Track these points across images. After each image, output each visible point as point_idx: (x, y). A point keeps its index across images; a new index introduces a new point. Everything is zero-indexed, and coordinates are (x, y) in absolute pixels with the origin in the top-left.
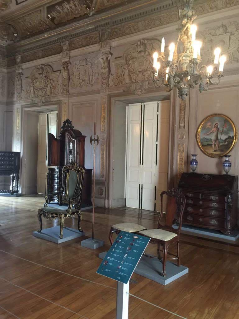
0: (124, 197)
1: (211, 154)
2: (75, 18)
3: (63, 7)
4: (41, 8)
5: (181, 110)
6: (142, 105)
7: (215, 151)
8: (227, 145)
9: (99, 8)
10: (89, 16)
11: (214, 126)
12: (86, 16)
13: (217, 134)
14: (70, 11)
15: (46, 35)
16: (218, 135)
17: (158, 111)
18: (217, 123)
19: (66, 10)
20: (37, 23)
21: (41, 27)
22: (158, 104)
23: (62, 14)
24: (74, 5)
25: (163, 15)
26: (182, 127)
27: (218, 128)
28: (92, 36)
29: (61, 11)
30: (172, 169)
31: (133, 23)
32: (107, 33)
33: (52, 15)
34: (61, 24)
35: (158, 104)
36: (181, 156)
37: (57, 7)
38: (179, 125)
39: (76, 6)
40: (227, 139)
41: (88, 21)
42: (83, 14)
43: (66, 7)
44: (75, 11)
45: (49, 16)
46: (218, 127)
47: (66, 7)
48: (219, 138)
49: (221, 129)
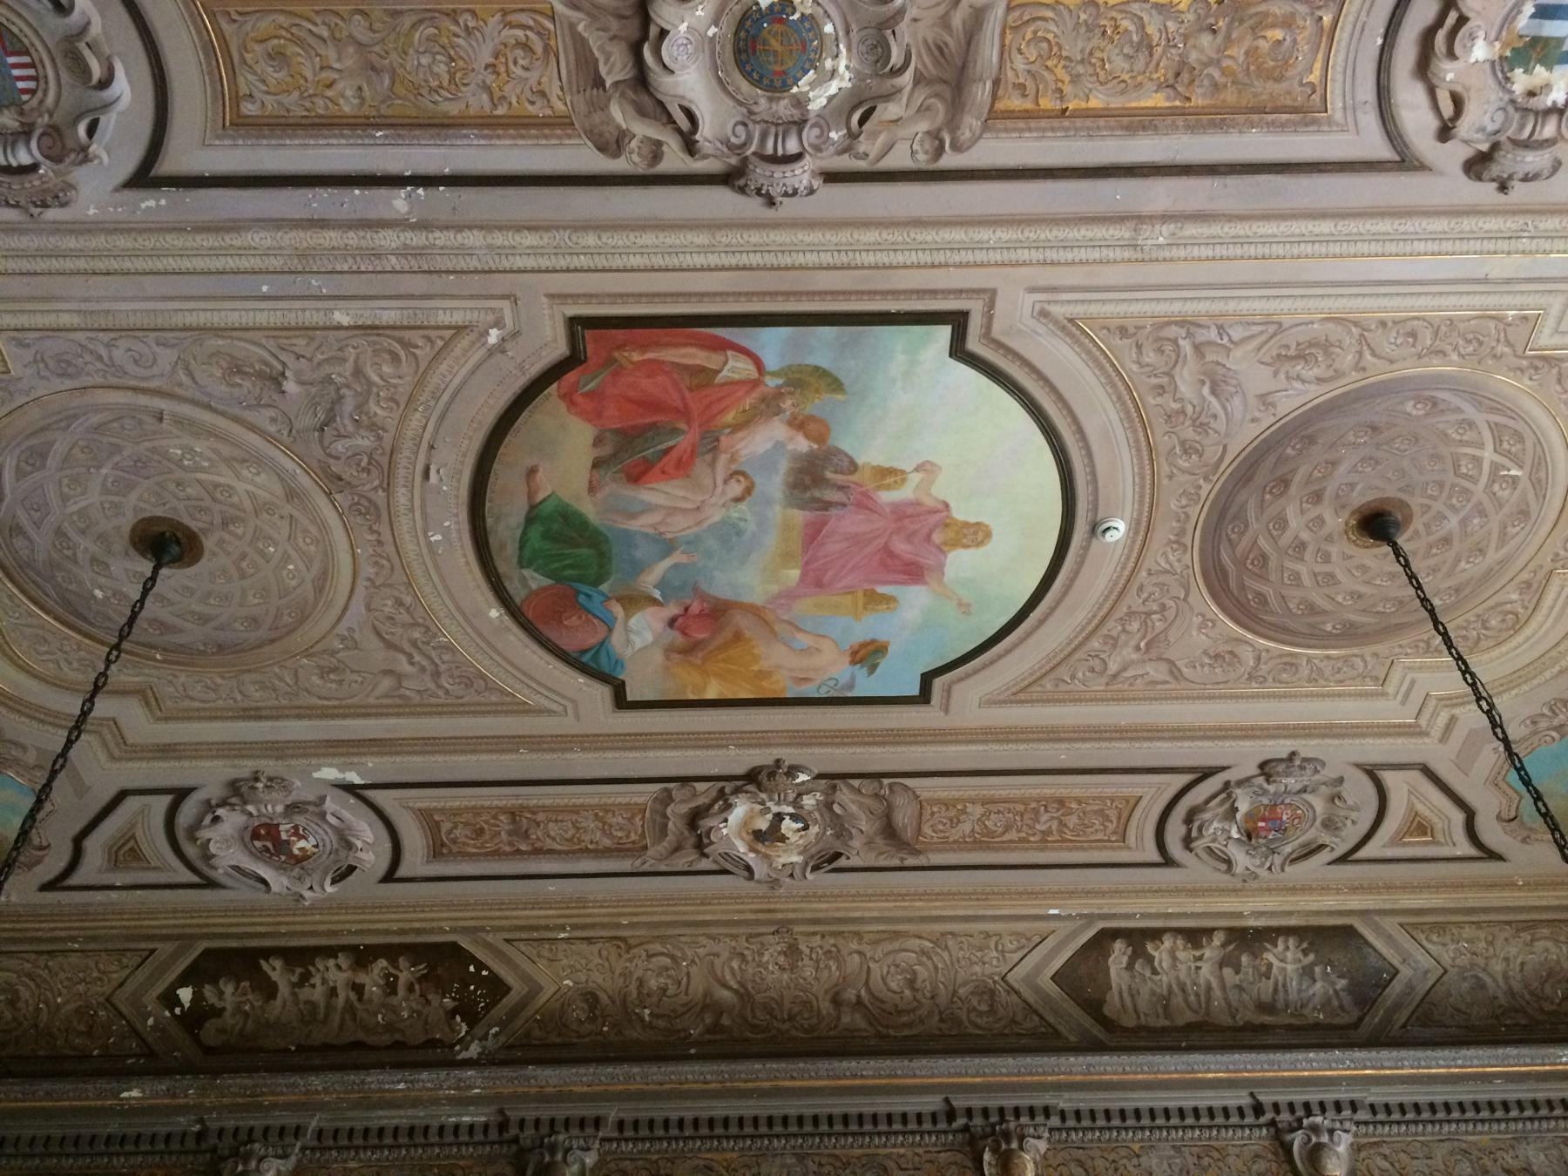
2: (359, 1045)
3: (305, 978)
4: (165, 949)
9: (528, 1034)
10: (459, 1057)
12: (429, 1053)
14: (340, 1001)
15: (135, 1093)
19: (317, 993)
20: (71, 1006)
21: (80, 1034)
23: (279, 1002)
24: (382, 982)
25: (901, 1156)
28: (462, 1163)
29: (284, 990)
31: (735, 1155)
32: (576, 1168)
33: (208, 991)
34: (250, 1053)
37: (275, 970)
39: (391, 987)
41: (479, 1082)
42: (423, 1039)
43: (324, 981)
44: (375, 1015)
45: (185, 994)
47: (324, 981)
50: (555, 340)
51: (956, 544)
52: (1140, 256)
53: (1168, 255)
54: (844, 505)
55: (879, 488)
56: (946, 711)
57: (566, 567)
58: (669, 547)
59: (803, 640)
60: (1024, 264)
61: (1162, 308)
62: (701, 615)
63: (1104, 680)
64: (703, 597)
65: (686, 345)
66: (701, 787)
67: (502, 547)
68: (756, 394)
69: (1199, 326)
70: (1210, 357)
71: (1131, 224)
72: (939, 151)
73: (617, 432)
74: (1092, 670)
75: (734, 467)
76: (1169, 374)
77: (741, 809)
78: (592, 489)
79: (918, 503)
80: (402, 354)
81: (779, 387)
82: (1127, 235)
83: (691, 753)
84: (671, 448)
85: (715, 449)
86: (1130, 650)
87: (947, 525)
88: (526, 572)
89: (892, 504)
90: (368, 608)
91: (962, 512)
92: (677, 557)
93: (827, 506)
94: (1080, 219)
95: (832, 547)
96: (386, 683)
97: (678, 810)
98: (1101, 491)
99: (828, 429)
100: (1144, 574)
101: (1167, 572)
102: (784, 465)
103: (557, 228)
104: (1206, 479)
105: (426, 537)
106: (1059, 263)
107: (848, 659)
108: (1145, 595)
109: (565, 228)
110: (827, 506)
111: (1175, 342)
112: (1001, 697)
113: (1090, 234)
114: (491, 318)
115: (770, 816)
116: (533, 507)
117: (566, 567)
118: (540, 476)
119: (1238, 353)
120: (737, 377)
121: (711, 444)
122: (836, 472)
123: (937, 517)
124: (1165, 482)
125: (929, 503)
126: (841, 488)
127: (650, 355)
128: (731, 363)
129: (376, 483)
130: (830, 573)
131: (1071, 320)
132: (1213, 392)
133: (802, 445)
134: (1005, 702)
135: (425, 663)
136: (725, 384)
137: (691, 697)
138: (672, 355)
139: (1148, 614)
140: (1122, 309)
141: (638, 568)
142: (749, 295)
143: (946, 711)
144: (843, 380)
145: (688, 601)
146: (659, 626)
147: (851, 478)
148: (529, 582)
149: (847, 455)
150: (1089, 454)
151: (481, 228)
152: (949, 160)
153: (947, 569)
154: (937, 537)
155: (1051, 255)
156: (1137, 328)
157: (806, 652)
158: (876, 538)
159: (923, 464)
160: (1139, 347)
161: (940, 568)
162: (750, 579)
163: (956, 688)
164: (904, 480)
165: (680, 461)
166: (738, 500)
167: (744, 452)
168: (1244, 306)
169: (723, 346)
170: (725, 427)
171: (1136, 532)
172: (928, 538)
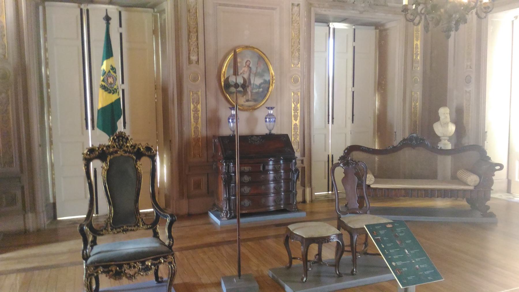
0: (47, 199)
1: (242, 105)
5: (189, 32)
6: (81, 10)
7: (248, 101)
8: (263, 92)
11: (245, 65)
13: (250, 75)
16: (251, 78)
17: (121, 26)
18: (249, 60)
22: (120, 13)
26: (194, 62)
27: (250, 68)
30: (181, 133)
35: (120, 13)
36: (196, 110)
38: (189, 58)
40: (260, 85)
46: (251, 66)
48: (252, 82)
49: (254, 69)
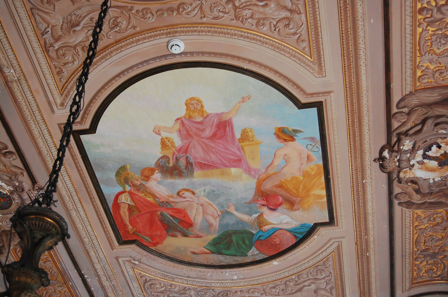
50: (131, 248)
51: (201, 111)
52: (22, 77)
53: (17, 67)
54: (187, 158)
55: (173, 146)
56: (329, 92)
57: (244, 242)
58: (225, 213)
59: (279, 161)
60: (42, 117)
61: (43, 61)
62: (267, 201)
63: (296, 16)
64: (254, 200)
65: (119, 214)
66: (397, 190)
67: (236, 261)
68: (136, 192)
69: (45, 43)
70: (61, 33)
71: (10, 84)
72: (10, 153)
73: (166, 230)
74: (287, 25)
75: (175, 196)
76: (75, 47)
77: (419, 173)
78: (198, 237)
79: (180, 131)
80: (150, 283)
81: (130, 186)
82: (15, 84)
83: (369, 196)
84: (171, 216)
85: (167, 202)
86: (267, 9)
87: (190, 117)
88: (250, 254)
89: (182, 141)
90: (279, 295)
91: (182, 112)
92: (232, 210)
93: (189, 164)
94: (16, 103)
95: (214, 158)
96: (323, 292)
97: (416, 198)
98: (151, 57)
99: (146, 168)
100: (205, 20)
101: (201, 7)
102: (170, 180)
103: (85, 248)
104: (131, 9)
105: (235, 280)
106: (37, 105)
107: (291, 143)
108: (221, 14)
109: (84, 246)
110: (189, 164)
111: (57, 50)
112: (316, 67)
113: (20, 98)
114: (127, 263)
115: (425, 161)
116: (213, 253)
117: (244, 242)
118: (195, 251)
119: (53, 22)
120: (129, 199)
121: (166, 204)
122: (169, 163)
123: (186, 122)
124: (138, 29)
125: (178, 126)
126: (177, 160)
127: (128, 223)
128: (123, 201)
129: (211, 291)
130: (230, 157)
131: (62, 95)
132: (78, 25)
133: (157, 175)
134: (320, 65)
135: (309, 282)
136: (134, 202)
137: (325, 199)
138: (127, 220)
139: (235, 8)
140: (49, 76)
141: (240, 222)
142: (91, 199)
143: (329, 92)
144: (120, 166)
145: (258, 205)
146: (275, 214)
147: (171, 157)
148: (254, 253)
149: (159, 160)
150: (131, 68)
151: (93, 265)
152: (11, 148)
153: (219, 112)
154: (199, 119)
155: (35, 108)
156: (56, 68)
157: (287, 159)
158: (204, 143)
159: (156, 133)
160: (65, 64)
161: (219, 115)
162: (240, 185)
163: (309, 91)
164: (167, 138)
165: (176, 213)
166: (193, 193)
167: (167, 194)
168: (29, 28)
169: (116, 205)
170: (156, 200)
171: (176, 32)
172: (198, 123)
